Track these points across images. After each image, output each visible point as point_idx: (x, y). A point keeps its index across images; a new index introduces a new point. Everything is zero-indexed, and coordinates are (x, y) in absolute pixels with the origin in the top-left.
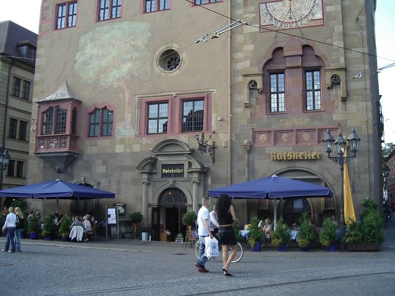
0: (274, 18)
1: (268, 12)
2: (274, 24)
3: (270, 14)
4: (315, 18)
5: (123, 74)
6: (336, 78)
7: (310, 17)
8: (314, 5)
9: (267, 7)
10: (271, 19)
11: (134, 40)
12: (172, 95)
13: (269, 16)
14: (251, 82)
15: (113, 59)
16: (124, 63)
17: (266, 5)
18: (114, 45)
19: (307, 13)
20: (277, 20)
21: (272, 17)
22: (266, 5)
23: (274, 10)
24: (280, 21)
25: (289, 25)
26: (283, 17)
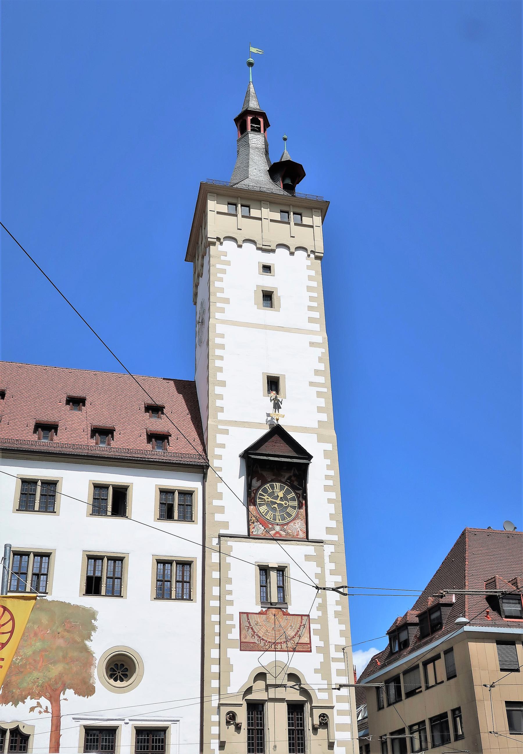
0: (257, 635)
1: (250, 625)
2: (257, 642)
3: (252, 628)
4: (301, 641)
5: (50, 679)
6: (324, 717)
7: (296, 639)
8: (301, 626)
9: (248, 619)
10: (253, 636)
11: (68, 631)
12: (124, 720)
13: (250, 630)
14: (228, 713)
15: (34, 653)
16: (51, 664)
17: (248, 616)
18: (36, 634)
19: (293, 634)
20: (260, 637)
21: (254, 632)
22: (248, 616)
23: (256, 624)
24: (263, 639)
25: (273, 646)
26: (267, 635)
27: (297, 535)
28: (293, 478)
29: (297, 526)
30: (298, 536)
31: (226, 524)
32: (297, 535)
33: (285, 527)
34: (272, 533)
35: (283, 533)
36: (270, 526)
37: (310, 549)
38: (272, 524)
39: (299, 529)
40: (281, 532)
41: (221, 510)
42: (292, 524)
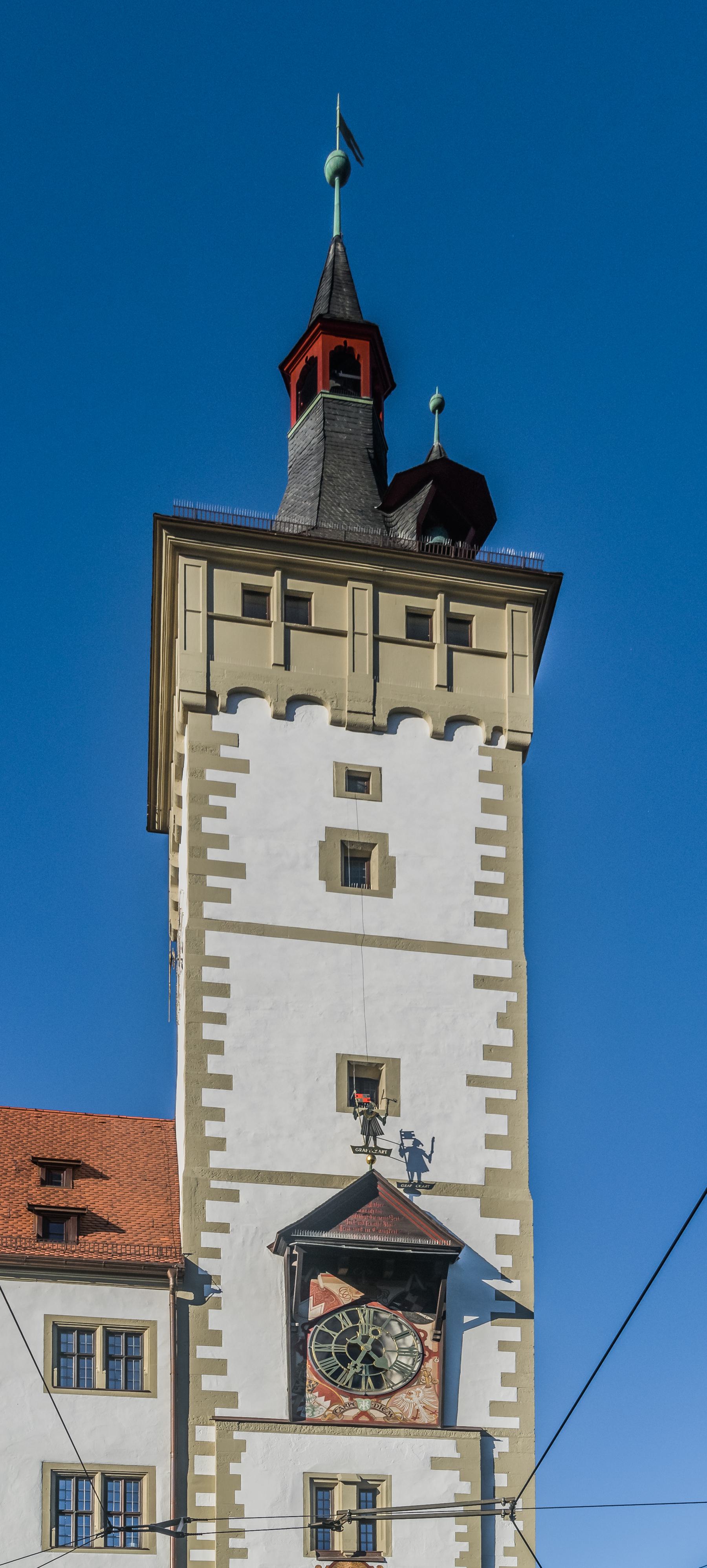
27: (415, 1418)
28: (409, 1298)
29: (415, 1399)
30: (418, 1421)
31: (231, 1399)
32: (415, 1418)
33: (384, 1402)
34: (350, 1414)
35: (378, 1415)
36: (346, 1400)
37: (445, 1446)
38: (352, 1397)
39: (420, 1406)
40: (373, 1412)
41: (219, 1367)
42: (402, 1395)
